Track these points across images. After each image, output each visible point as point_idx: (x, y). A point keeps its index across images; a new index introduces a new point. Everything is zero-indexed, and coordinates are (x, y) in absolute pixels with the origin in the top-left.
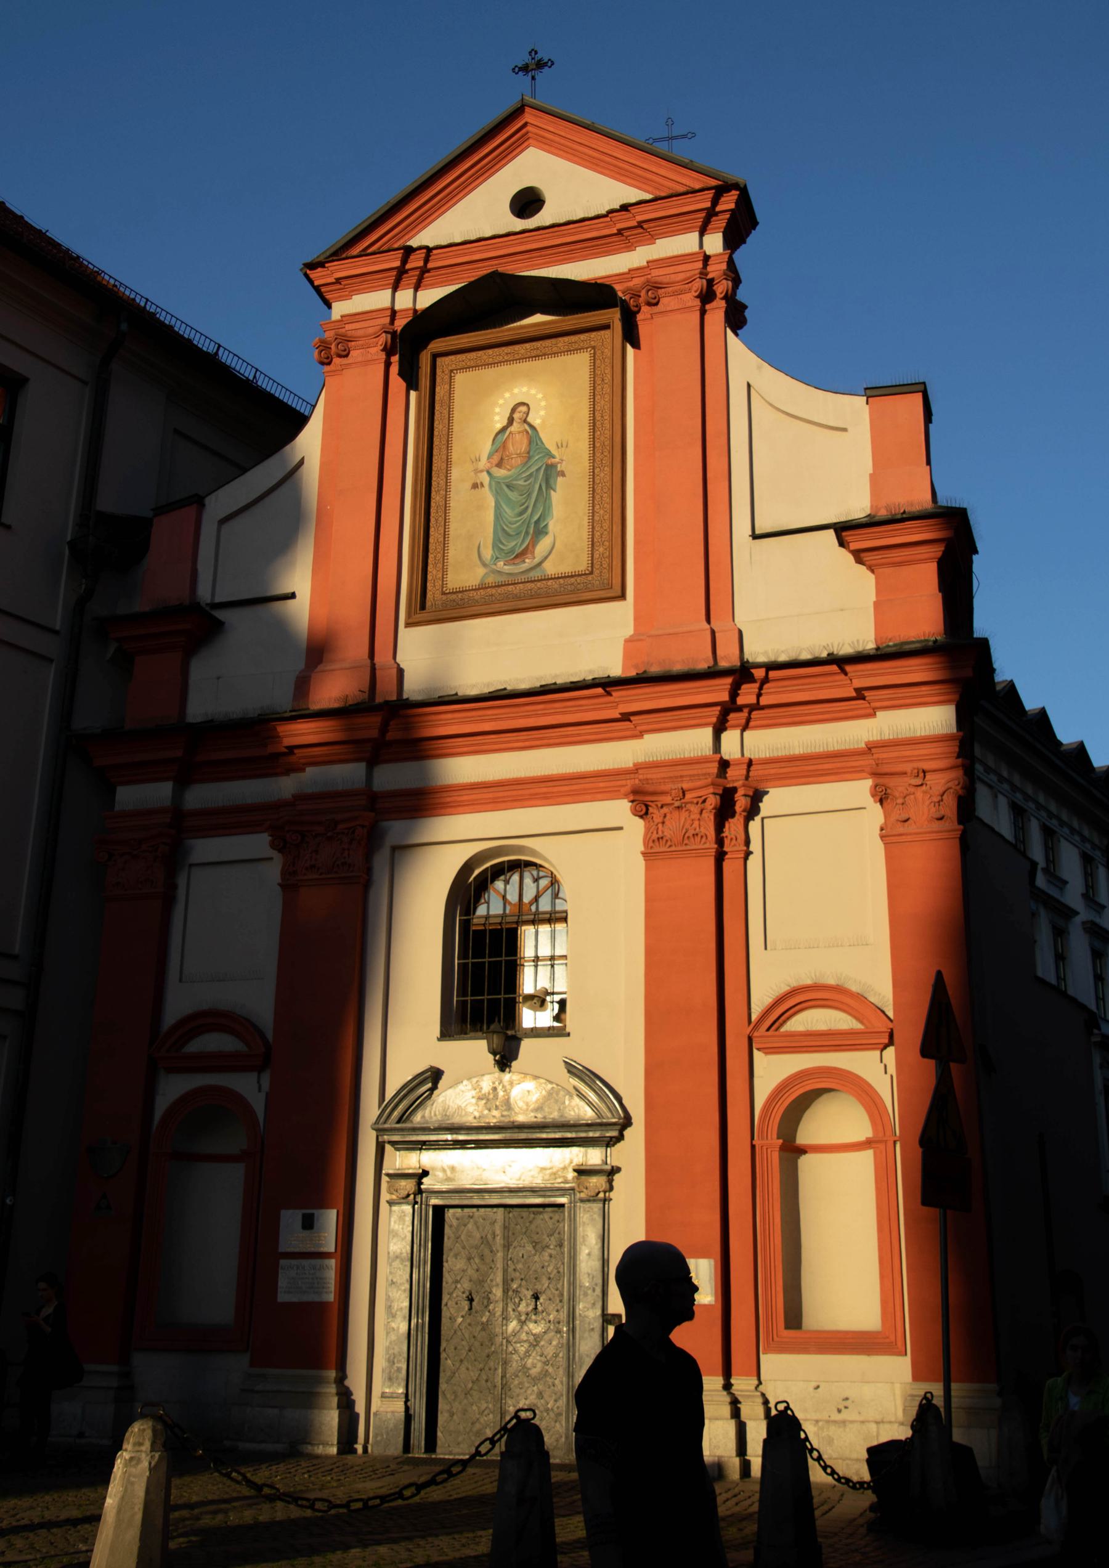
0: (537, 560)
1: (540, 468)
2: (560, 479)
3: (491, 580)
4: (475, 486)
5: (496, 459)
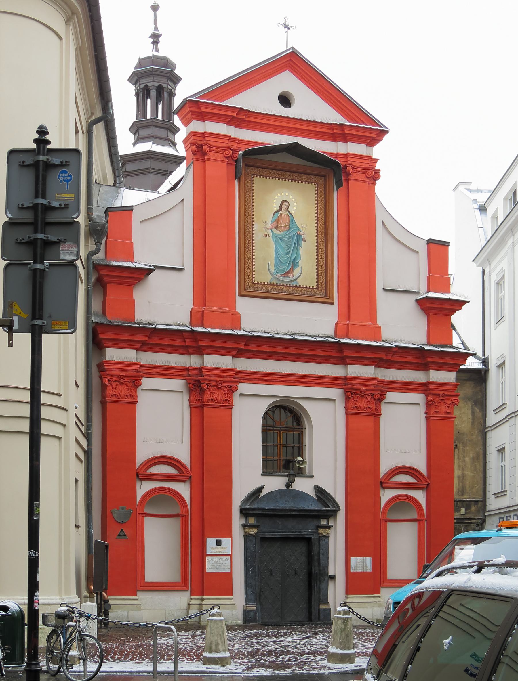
0: (294, 278)
1: (294, 235)
2: (303, 242)
3: (274, 282)
4: (265, 235)
5: (275, 225)
